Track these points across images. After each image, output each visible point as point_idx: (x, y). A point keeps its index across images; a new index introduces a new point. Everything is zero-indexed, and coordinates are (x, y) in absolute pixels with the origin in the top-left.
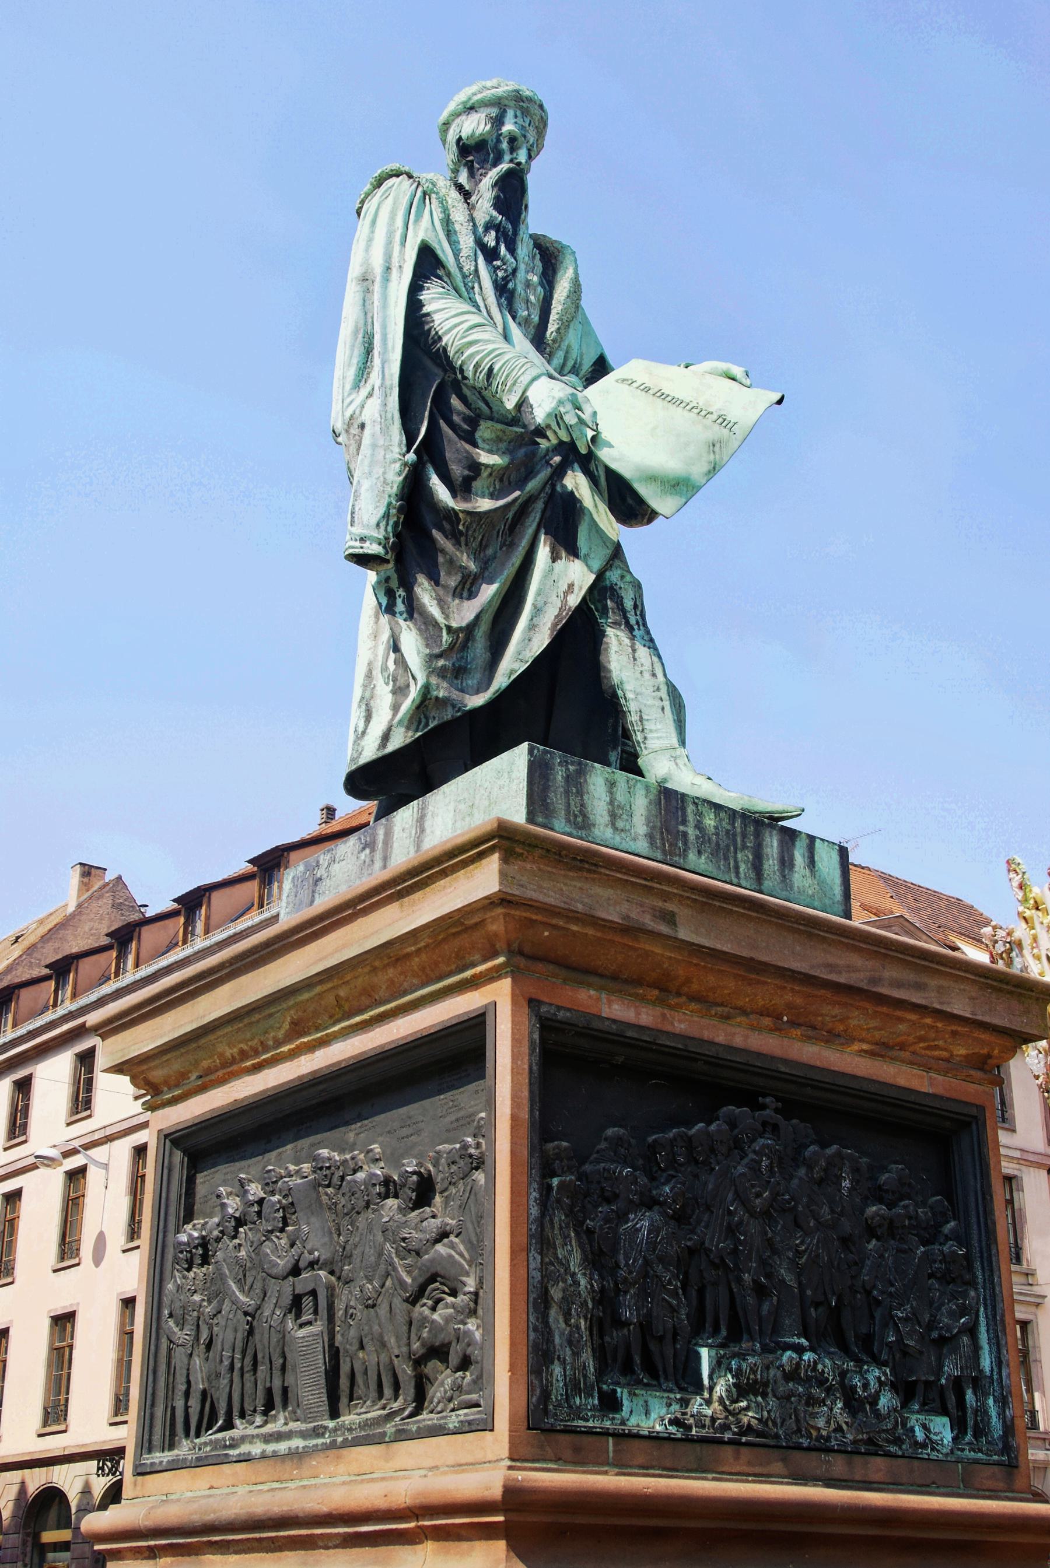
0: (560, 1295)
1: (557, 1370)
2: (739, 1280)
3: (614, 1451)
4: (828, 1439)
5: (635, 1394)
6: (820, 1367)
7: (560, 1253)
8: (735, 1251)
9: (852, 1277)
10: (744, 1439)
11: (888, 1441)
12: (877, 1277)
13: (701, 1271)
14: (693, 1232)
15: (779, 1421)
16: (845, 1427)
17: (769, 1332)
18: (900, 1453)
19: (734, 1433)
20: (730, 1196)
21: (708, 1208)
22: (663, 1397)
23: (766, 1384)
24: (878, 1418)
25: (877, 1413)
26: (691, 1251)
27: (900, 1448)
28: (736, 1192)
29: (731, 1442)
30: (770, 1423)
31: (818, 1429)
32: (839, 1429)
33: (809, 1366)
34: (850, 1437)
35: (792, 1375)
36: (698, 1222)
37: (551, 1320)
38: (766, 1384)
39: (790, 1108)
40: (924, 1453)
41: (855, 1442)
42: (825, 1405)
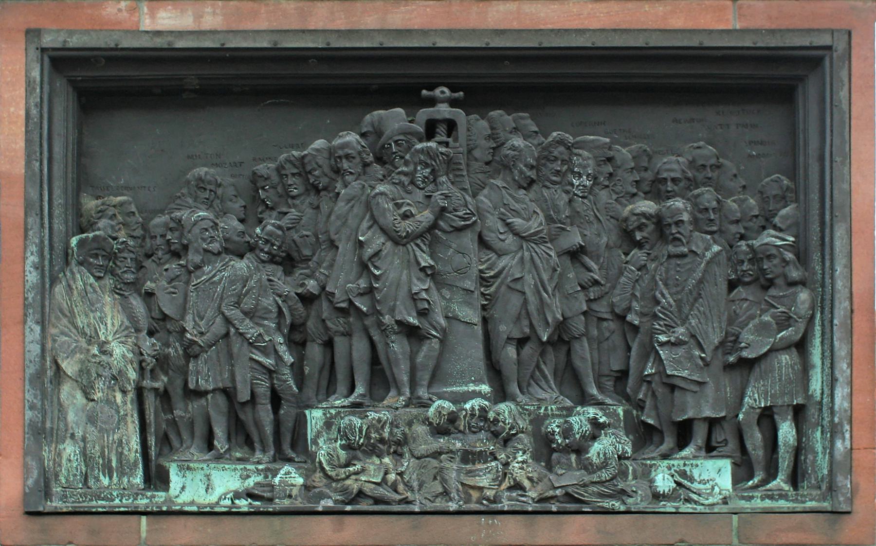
0: (76, 368)
1: (69, 449)
2: (380, 324)
3: (147, 531)
4: (495, 500)
5: (189, 468)
6: (491, 415)
7: (80, 321)
8: (370, 291)
9: (589, 301)
10: (348, 508)
11: (602, 495)
12: (633, 295)
13: (324, 321)
14: (309, 277)
15: (415, 484)
16: (526, 484)
17: (425, 383)
18: (622, 508)
19: (336, 502)
20: (365, 224)
21: (333, 245)
22: (235, 469)
23: (403, 442)
24: (585, 468)
25: (588, 467)
26: (307, 299)
27: (624, 503)
28: (374, 221)
29: (327, 512)
30: (401, 487)
31: (481, 489)
32: (517, 486)
33: (473, 415)
34: (533, 494)
35: (445, 427)
36: (319, 264)
37: (63, 396)
38: (403, 442)
39: (477, 96)
40: (670, 507)
41: (542, 500)
42: (496, 459)
